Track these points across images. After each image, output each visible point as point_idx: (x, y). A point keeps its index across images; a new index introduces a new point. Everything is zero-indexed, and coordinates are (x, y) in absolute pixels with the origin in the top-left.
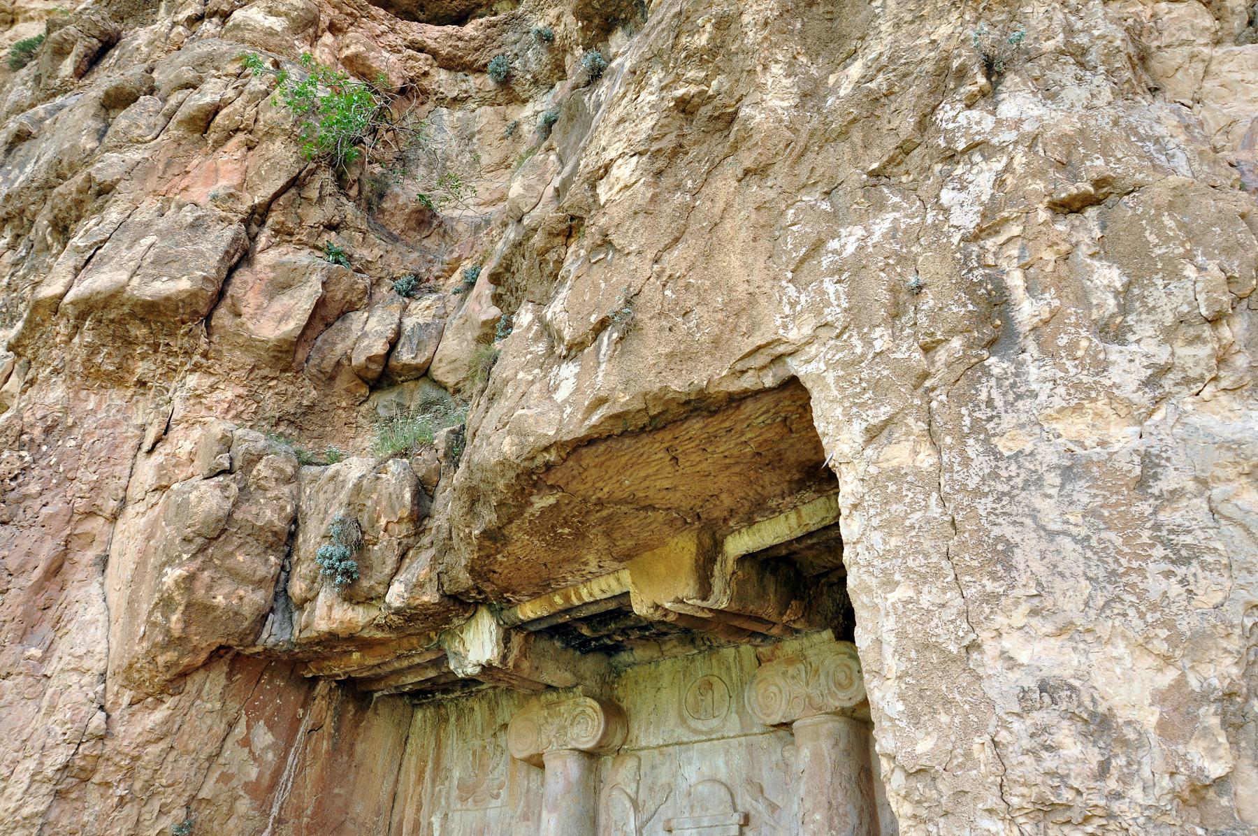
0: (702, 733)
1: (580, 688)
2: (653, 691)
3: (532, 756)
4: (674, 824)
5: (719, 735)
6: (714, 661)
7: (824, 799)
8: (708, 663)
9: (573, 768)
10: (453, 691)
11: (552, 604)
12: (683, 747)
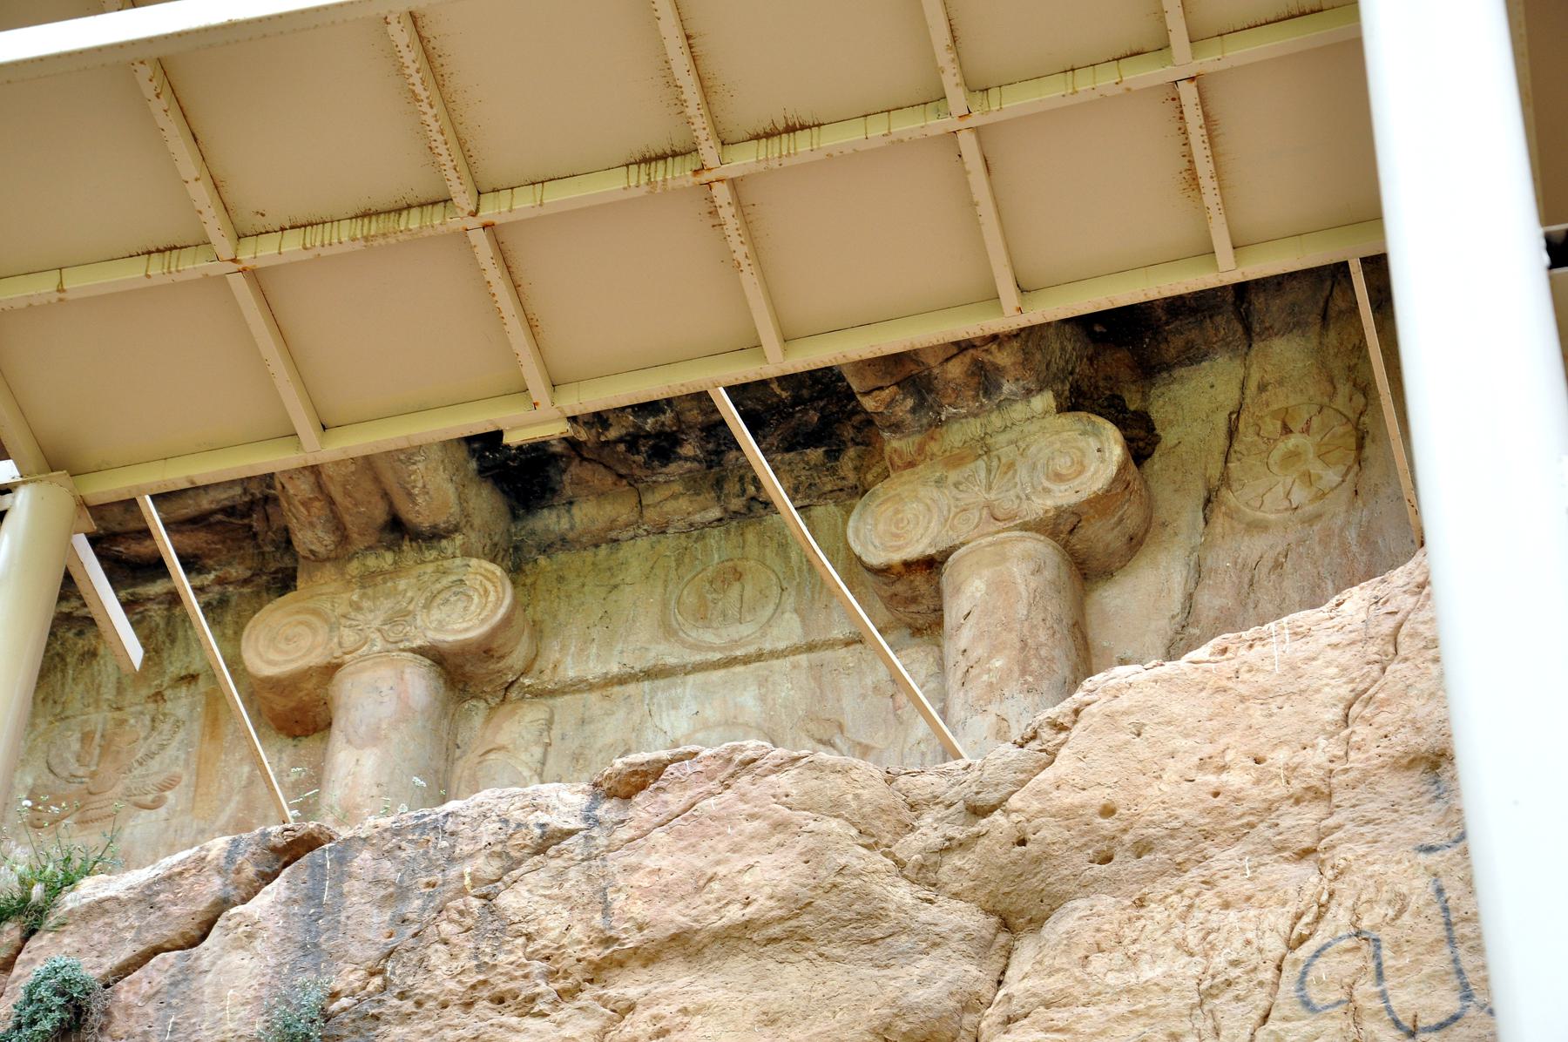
0: (712, 648)
1: (459, 539)
3: (306, 674)
5: (752, 649)
6: (751, 536)
7: (1013, 638)
8: (735, 538)
9: (419, 683)
12: (661, 683)
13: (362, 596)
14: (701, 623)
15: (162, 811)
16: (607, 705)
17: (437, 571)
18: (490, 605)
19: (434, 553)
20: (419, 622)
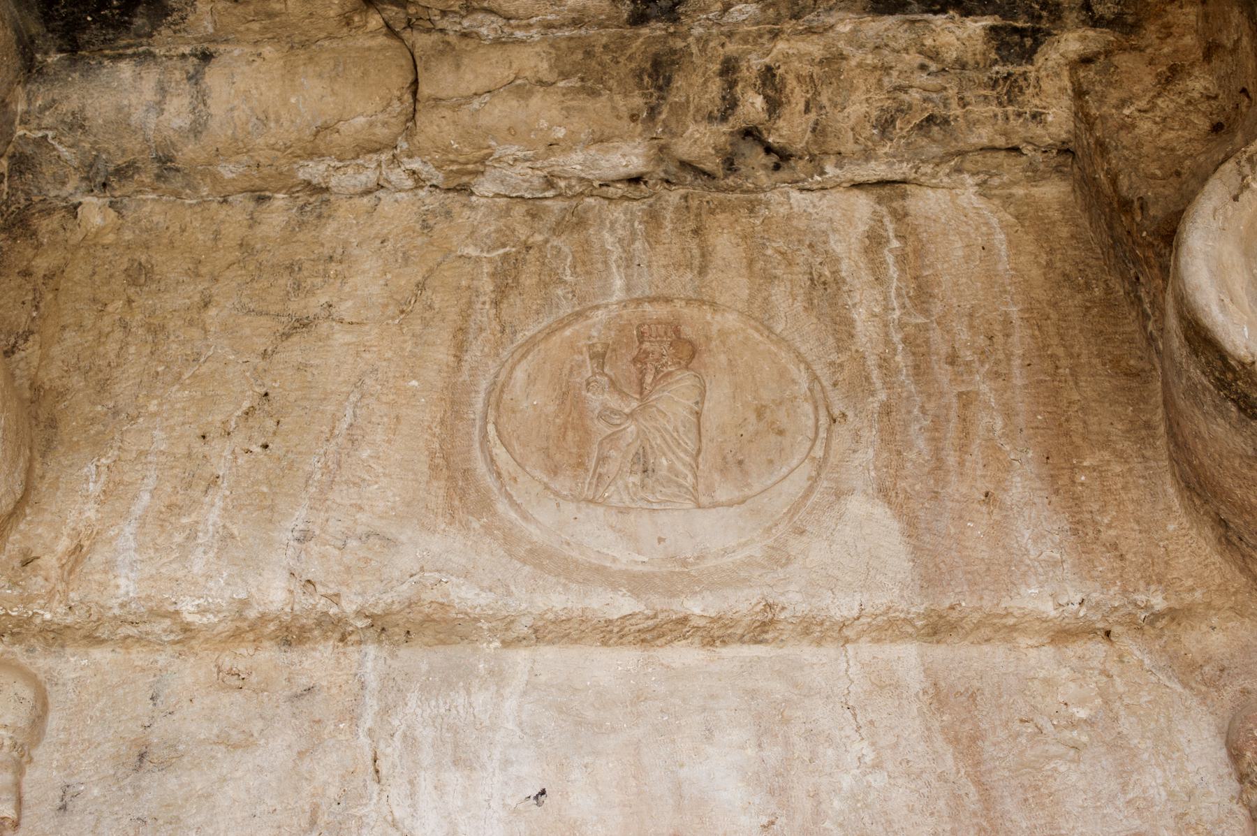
2: (259, 332)
5: (742, 603)
6: (724, 243)
12: (419, 659)
14: (563, 483)
16: (232, 705)
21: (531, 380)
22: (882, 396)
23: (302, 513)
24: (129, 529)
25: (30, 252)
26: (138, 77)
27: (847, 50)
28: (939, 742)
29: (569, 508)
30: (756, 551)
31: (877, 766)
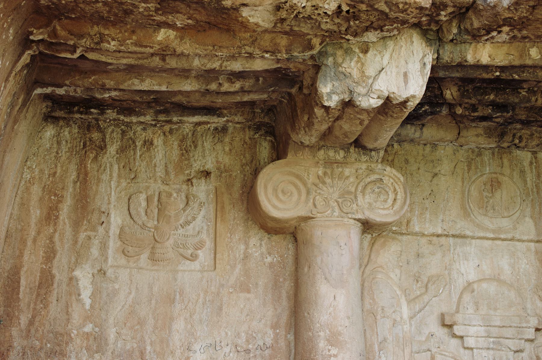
2: (429, 176)
4: (459, 318)
5: (509, 236)
6: (505, 161)
10: (139, 114)
11: (524, 53)
13: (325, 174)
14: (481, 211)
15: (197, 263)
17: (367, 169)
18: (399, 203)
19: (367, 158)
20: (360, 204)
21: (474, 189)
22: (532, 197)
23: (441, 216)
24: (416, 218)
25: (387, 156)
26: (411, 128)
27: (534, 133)
28: (537, 261)
29: (483, 217)
30: (511, 226)
31: (528, 264)
